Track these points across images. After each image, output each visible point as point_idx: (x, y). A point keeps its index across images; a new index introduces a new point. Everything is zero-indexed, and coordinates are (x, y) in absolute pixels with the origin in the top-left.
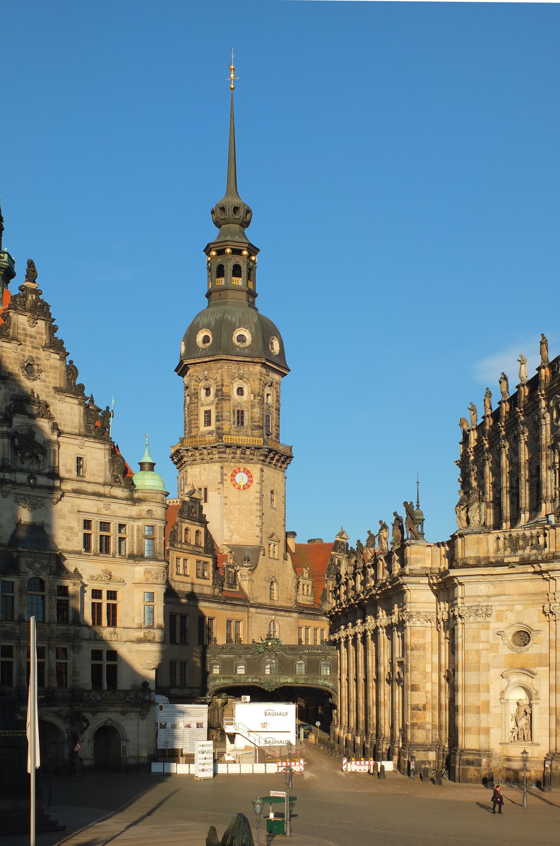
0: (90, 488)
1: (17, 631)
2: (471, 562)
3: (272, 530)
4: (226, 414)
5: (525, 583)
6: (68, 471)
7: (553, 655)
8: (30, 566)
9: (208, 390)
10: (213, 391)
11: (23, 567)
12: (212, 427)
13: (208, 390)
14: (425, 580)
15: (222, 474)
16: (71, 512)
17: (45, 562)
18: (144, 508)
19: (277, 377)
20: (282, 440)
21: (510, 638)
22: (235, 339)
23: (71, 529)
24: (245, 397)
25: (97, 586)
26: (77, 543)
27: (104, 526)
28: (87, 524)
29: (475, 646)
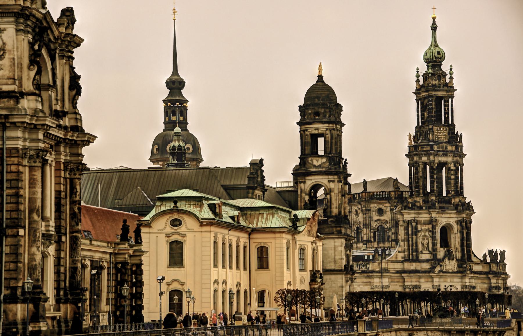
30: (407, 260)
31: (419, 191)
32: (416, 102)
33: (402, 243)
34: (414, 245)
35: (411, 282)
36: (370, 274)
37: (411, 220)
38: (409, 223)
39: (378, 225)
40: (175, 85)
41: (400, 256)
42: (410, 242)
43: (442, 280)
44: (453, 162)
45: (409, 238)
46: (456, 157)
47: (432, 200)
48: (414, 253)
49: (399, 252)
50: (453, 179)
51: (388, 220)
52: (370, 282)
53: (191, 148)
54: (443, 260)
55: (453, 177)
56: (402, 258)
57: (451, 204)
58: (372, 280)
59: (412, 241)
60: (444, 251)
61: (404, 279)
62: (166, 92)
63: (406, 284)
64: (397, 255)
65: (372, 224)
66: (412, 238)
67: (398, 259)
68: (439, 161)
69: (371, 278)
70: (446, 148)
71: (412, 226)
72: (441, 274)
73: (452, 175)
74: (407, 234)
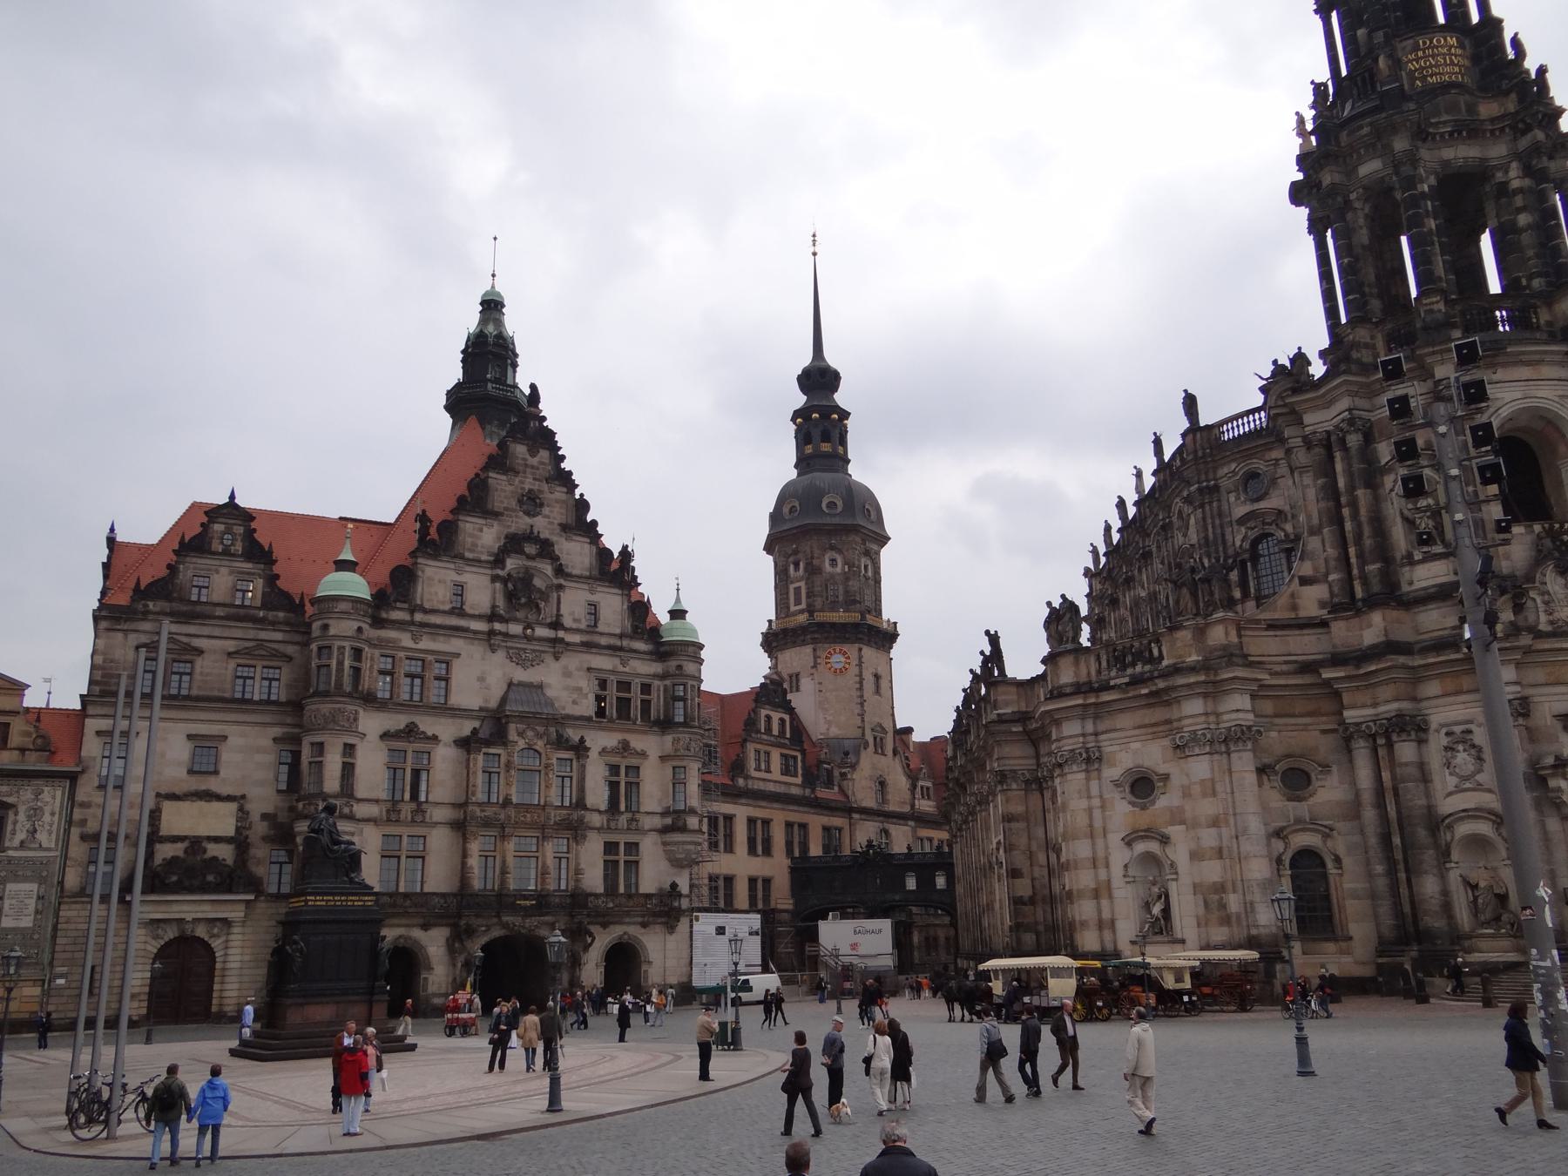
0: (604, 641)
1: (502, 816)
2: (1068, 690)
3: (877, 720)
4: (817, 589)
5: (1141, 713)
6: (575, 620)
7: (1187, 808)
8: (521, 734)
9: (797, 565)
10: (802, 565)
11: (512, 735)
12: (803, 606)
13: (797, 565)
14: (1017, 728)
15: (815, 657)
16: (579, 669)
17: (541, 729)
18: (673, 664)
19: (875, 547)
20: (885, 617)
21: (1128, 789)
22: (824, 506)
23: (580, 689)
24: (839, 569)
25: (615, 760)
26: (587, 707)
27: (624, 686)
28: (603, 684)
29: (1084, 804)
30: (1346, 605)
31: (1366, 303)
32: (1317, 22)
33: (1314, 543)
34: (1367, 531)
35: (1375, 705)
36: (1161, 684)
37: (1337, 427)
38: (1328, 444)
39: (1252, 534)
40: (819, 380)
41: (1311, 600)
42: (1348, 526)
43: (1538, 675)
44: (1516, 156)
45: (1339, 506)
46: (1529, 129)
47: (1432, 311)
48: (1373, 568)
49: (1305, 581)
50: (1529, 227)
51: (1287, 508)
52: (1168, 722)
53: (840, 504)
54: (1530, 578)
55: (1523, 219)
56: (1322, 604)
57: (1538, 328)
58: (1174, 713)
59: (1355, 515)
60: (1529, 538)
61: (1337, 695)
62: (800, 400)
63: (1350, 715)
64: (1293, 595)
65: (1229, 537)
66: (1354, 504)
67: (1302, 614)
68: (1445, 163)
69: (1168, 703)
70: (1472, 109)
71: (1347, 458)
72: (1525, 640)
73: (1519, 210)
74: (1331, 492)
